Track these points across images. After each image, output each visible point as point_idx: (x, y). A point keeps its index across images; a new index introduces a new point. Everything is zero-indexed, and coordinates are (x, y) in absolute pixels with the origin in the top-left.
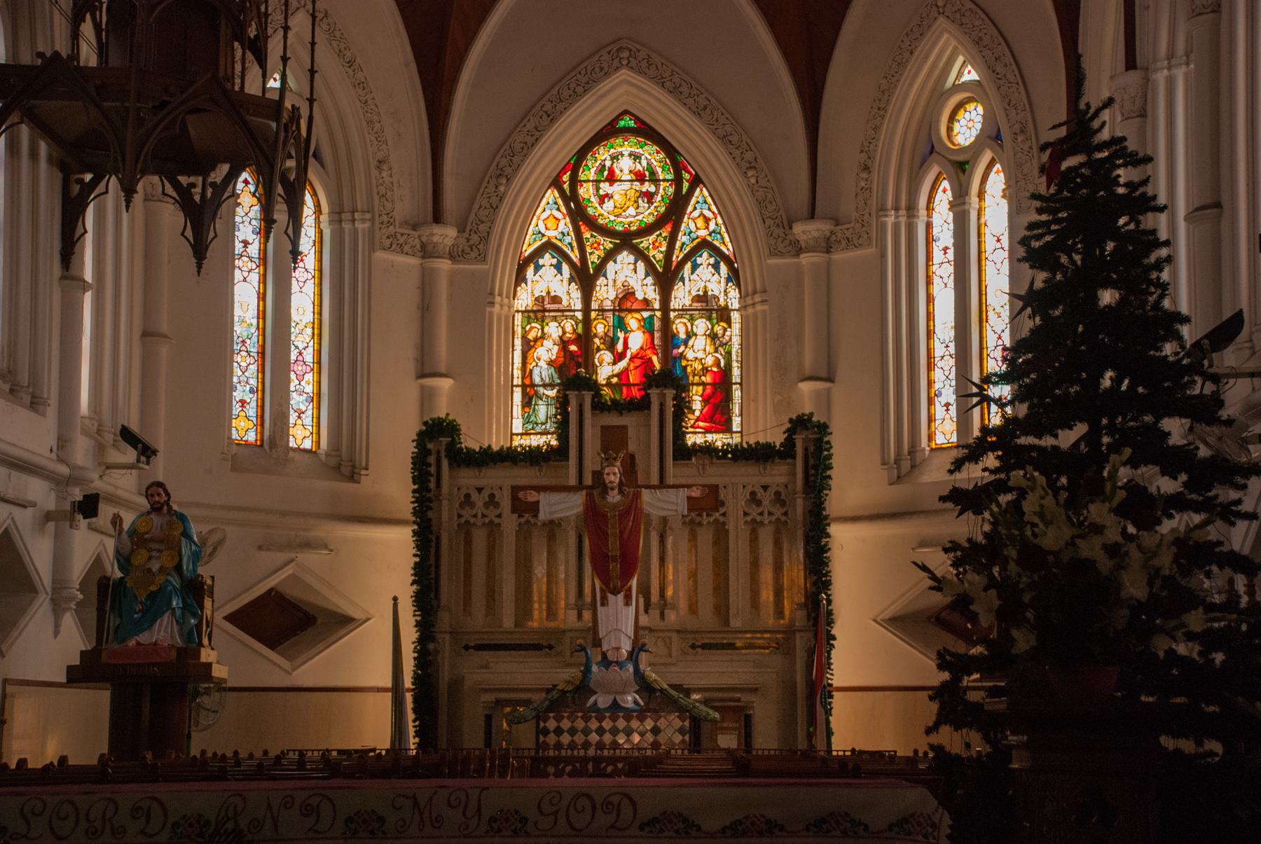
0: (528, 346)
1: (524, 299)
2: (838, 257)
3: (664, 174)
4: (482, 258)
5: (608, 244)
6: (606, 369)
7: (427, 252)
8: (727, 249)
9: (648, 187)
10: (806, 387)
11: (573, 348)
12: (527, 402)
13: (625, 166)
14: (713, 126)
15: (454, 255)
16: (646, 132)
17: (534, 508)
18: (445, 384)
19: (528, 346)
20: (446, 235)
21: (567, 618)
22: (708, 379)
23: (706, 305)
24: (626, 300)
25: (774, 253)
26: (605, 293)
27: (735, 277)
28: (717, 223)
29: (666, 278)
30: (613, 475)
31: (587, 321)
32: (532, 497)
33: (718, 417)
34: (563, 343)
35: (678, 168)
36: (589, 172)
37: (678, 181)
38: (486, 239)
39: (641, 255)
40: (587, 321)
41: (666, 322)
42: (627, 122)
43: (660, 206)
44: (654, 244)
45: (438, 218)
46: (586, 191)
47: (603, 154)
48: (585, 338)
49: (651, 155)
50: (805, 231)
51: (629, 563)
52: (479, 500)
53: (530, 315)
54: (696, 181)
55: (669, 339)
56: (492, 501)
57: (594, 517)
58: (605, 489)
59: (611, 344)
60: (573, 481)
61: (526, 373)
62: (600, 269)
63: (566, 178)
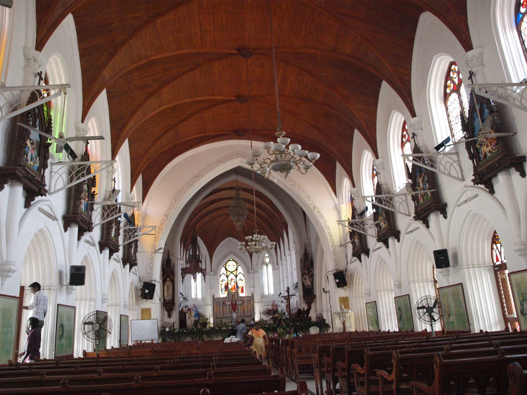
0: (221, 285)
1: (221, 279)
2: (255, 274)
3: (236, 265)
4: (216, 275)
5: (230, 273)
6: (230, 287)
7: (210, 275)
8: (243, 273)
9: (234, 266)
10: (252, 288)
11: (226, 285)
12: (222, 291)
13: (231, 265)
14: (241, 260)
15: (213, 275)
16: (233, 260)
17: (226, 303)
18: (213, 290)
19: (221, 285)
20: (212, 273)
21: (228, 315)
22: (241, 287)
23: (241, 280)
24: (232, 279)
25: (248, 274)
26: (230, 278)
27: (244, 276)
28: (242, 270)
29: (236, 276)
30: (234, 300)
31: (228, 282)
32: (225, 302)
33: (242, 292)
34: (225, 284)
35: (237, 264)
36: (227, 265)
37: (237, 266)
38: (217, 273)
39: (233, 274)
40: (228, 282)
41: (236, 281)
42: (231, 259)
43: (235, 269)
44: (235, 273)
45: (211, 271)
46: (227, 267)
47: (228, 263)
48: (227, 283)
49: (234, 263)
50: (251, 271)
51: (236, 310)
52: (218, 303)
53: (221, 281)
54: (239, 266)
55: (237, 283)
56: (219, 303)
57: (232, 304)
58: (233, 301)
59: (230, 284)
60: (228, 300)
61: (221, 288)
62: (229, 276)
63: (225, 266)
